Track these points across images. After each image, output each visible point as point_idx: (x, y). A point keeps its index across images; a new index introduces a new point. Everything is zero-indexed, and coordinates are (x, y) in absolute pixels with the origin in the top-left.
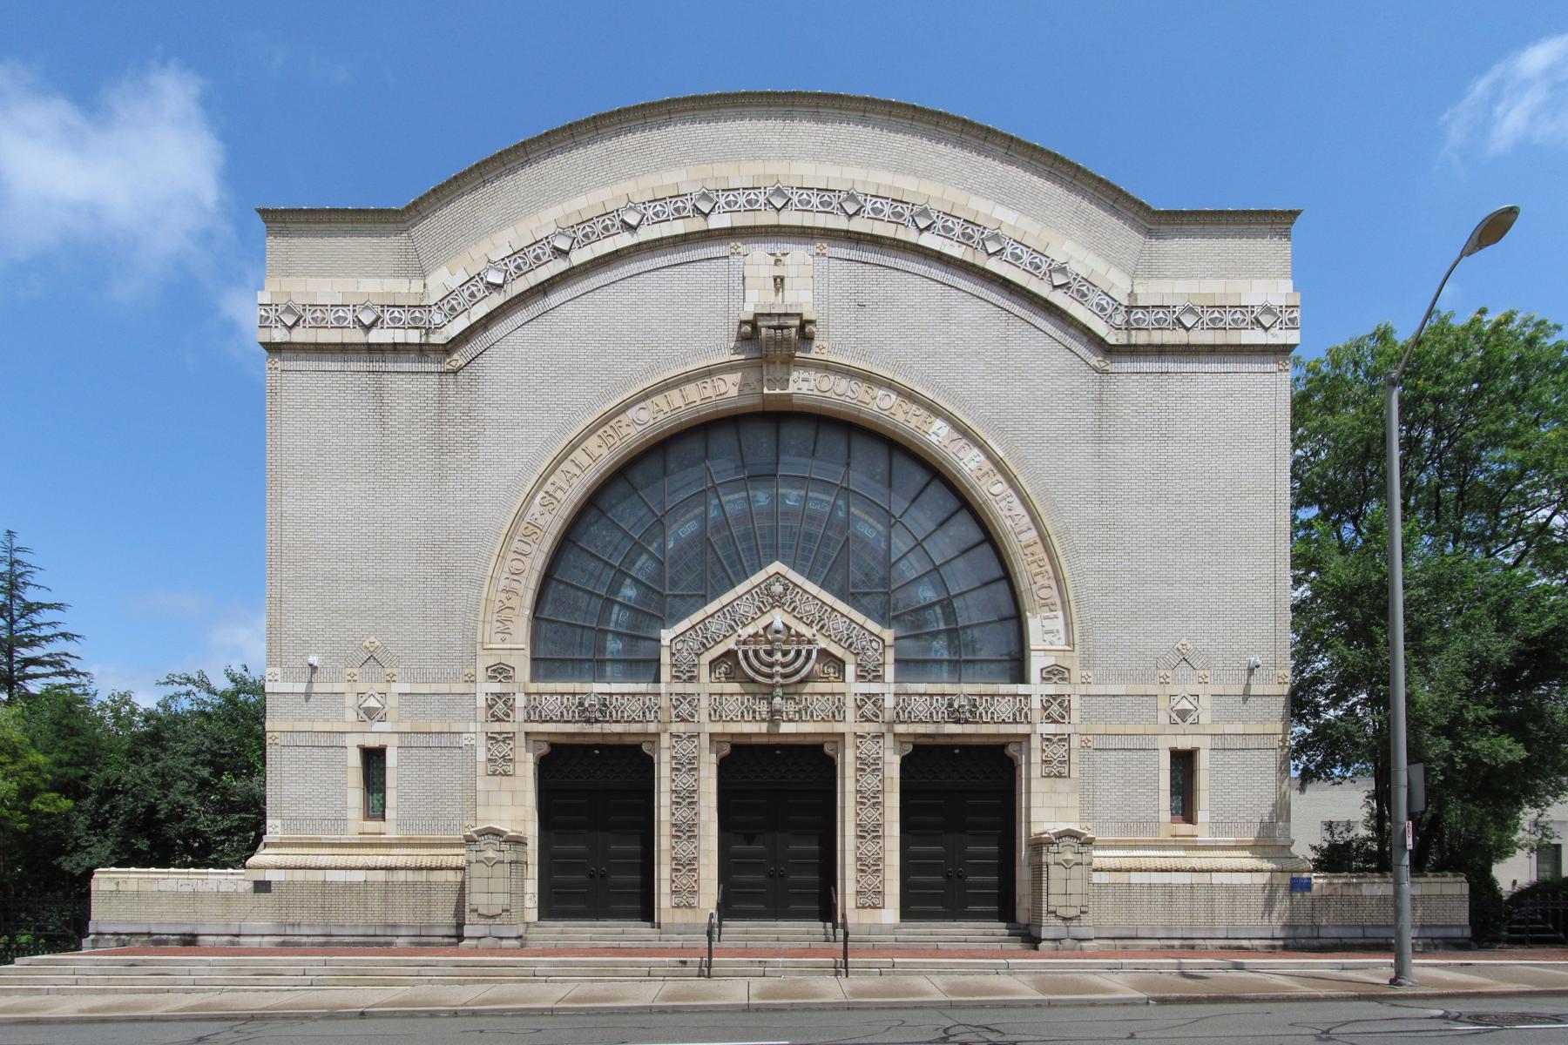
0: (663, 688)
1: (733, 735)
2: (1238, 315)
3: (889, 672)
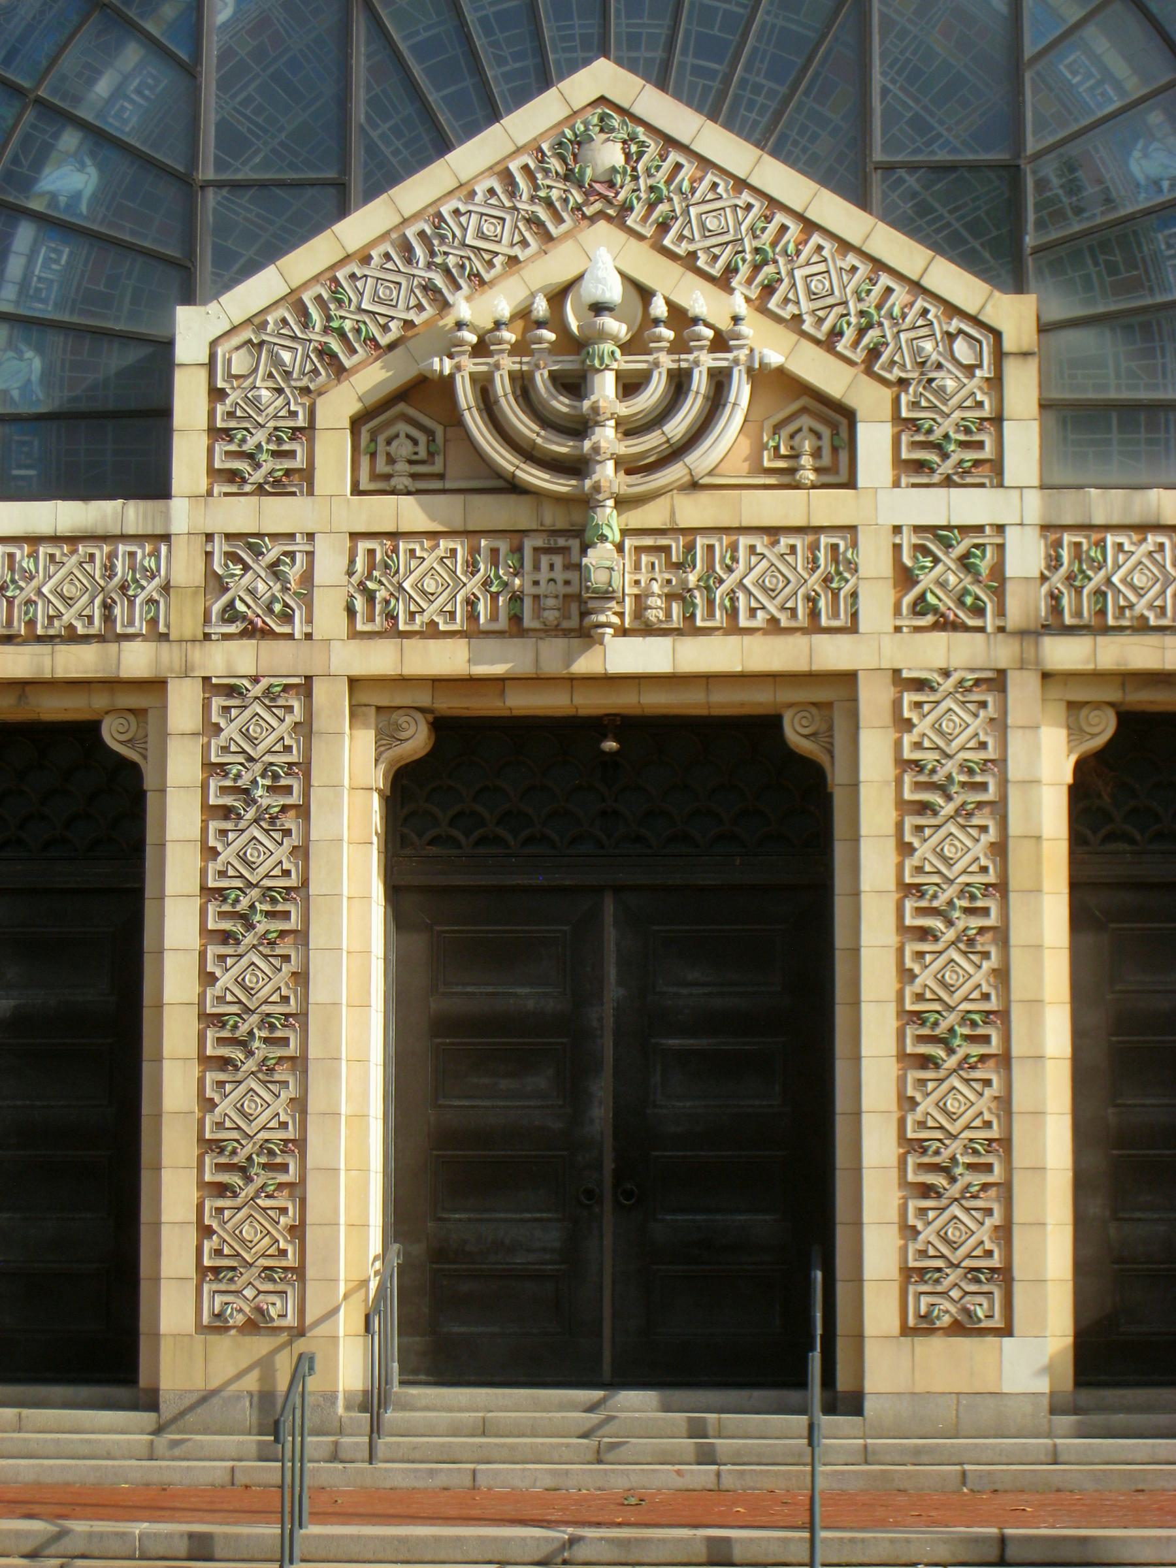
1: (437, 683)
3: (1023, 444)
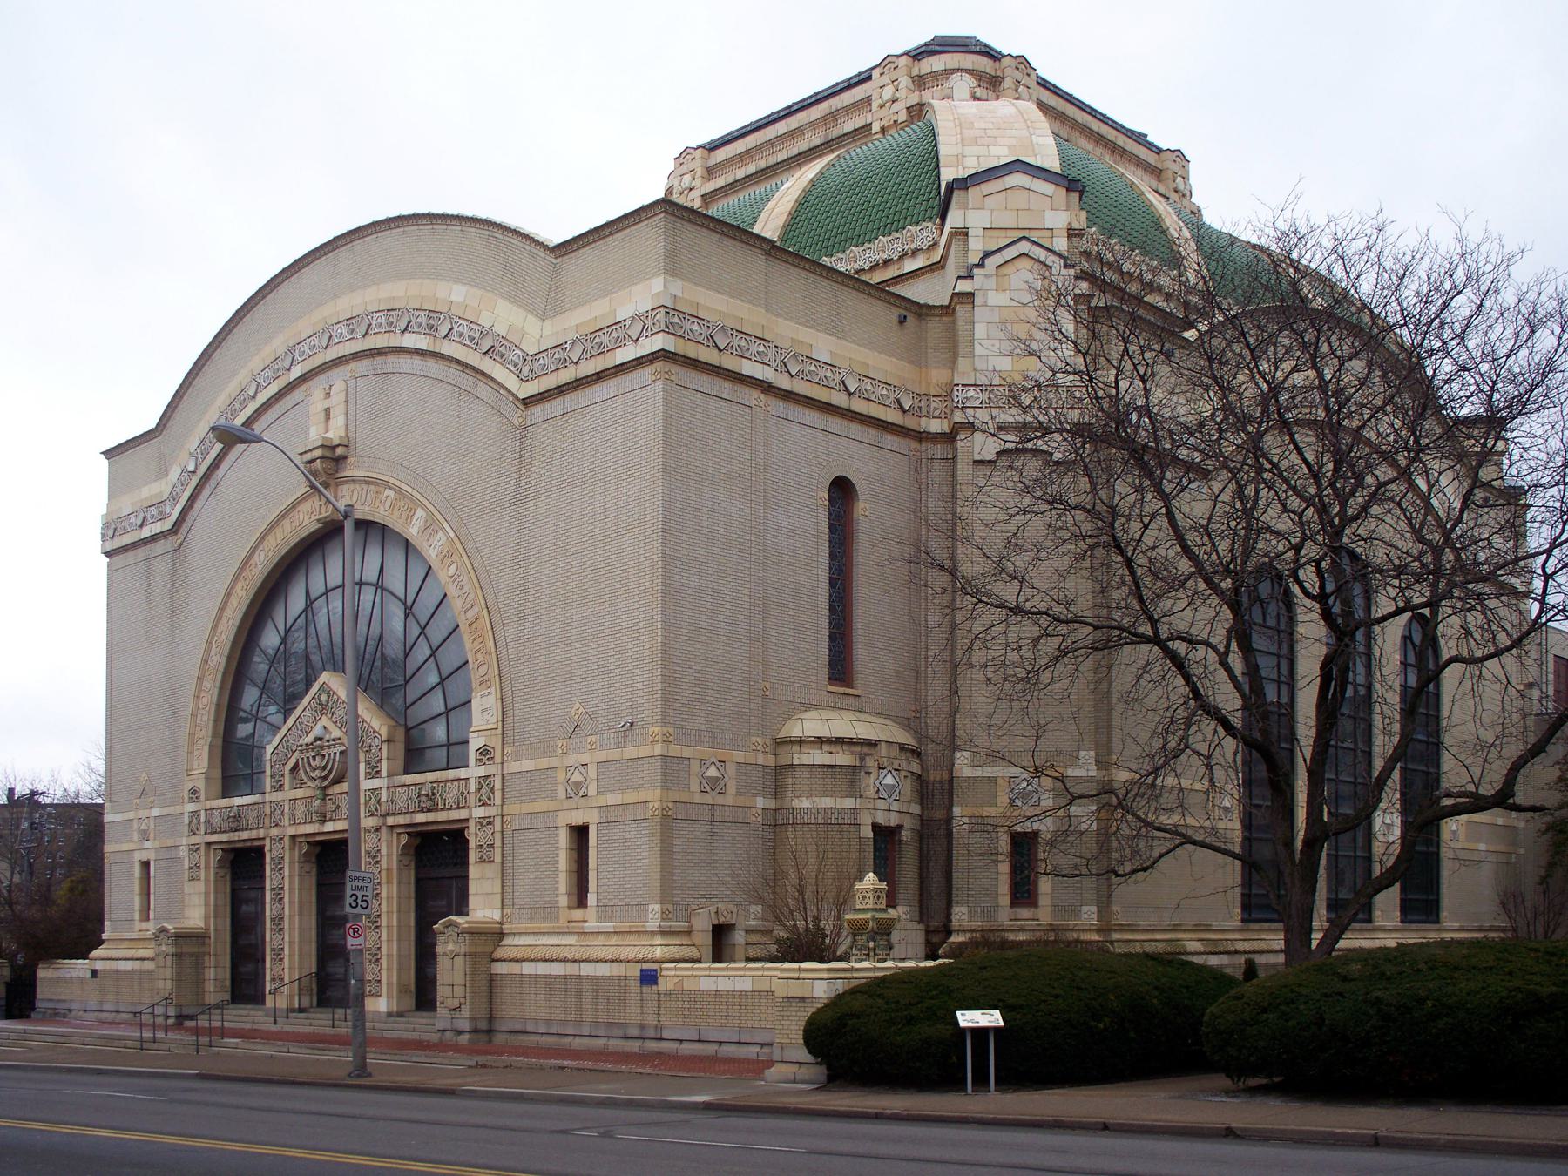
0: (268, 797)
2: (615, 334)
